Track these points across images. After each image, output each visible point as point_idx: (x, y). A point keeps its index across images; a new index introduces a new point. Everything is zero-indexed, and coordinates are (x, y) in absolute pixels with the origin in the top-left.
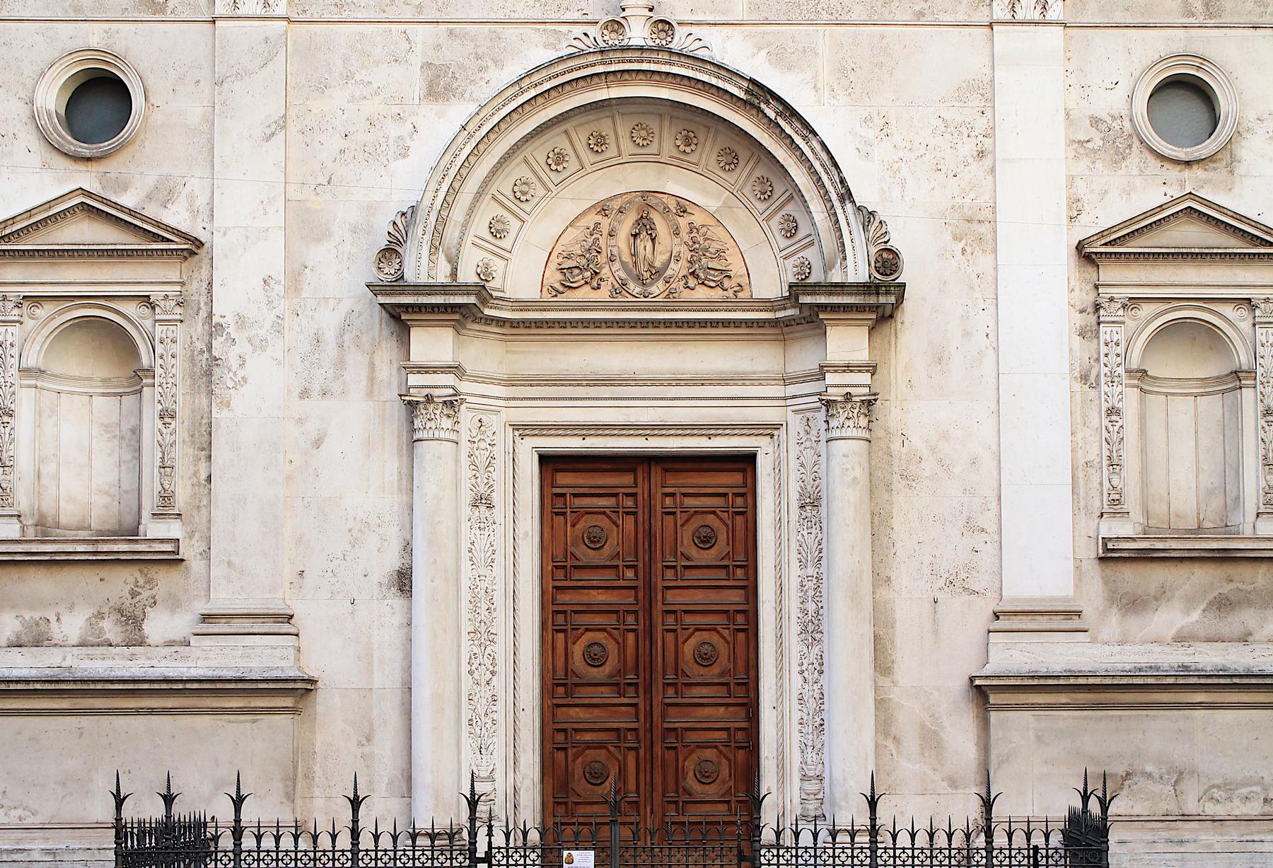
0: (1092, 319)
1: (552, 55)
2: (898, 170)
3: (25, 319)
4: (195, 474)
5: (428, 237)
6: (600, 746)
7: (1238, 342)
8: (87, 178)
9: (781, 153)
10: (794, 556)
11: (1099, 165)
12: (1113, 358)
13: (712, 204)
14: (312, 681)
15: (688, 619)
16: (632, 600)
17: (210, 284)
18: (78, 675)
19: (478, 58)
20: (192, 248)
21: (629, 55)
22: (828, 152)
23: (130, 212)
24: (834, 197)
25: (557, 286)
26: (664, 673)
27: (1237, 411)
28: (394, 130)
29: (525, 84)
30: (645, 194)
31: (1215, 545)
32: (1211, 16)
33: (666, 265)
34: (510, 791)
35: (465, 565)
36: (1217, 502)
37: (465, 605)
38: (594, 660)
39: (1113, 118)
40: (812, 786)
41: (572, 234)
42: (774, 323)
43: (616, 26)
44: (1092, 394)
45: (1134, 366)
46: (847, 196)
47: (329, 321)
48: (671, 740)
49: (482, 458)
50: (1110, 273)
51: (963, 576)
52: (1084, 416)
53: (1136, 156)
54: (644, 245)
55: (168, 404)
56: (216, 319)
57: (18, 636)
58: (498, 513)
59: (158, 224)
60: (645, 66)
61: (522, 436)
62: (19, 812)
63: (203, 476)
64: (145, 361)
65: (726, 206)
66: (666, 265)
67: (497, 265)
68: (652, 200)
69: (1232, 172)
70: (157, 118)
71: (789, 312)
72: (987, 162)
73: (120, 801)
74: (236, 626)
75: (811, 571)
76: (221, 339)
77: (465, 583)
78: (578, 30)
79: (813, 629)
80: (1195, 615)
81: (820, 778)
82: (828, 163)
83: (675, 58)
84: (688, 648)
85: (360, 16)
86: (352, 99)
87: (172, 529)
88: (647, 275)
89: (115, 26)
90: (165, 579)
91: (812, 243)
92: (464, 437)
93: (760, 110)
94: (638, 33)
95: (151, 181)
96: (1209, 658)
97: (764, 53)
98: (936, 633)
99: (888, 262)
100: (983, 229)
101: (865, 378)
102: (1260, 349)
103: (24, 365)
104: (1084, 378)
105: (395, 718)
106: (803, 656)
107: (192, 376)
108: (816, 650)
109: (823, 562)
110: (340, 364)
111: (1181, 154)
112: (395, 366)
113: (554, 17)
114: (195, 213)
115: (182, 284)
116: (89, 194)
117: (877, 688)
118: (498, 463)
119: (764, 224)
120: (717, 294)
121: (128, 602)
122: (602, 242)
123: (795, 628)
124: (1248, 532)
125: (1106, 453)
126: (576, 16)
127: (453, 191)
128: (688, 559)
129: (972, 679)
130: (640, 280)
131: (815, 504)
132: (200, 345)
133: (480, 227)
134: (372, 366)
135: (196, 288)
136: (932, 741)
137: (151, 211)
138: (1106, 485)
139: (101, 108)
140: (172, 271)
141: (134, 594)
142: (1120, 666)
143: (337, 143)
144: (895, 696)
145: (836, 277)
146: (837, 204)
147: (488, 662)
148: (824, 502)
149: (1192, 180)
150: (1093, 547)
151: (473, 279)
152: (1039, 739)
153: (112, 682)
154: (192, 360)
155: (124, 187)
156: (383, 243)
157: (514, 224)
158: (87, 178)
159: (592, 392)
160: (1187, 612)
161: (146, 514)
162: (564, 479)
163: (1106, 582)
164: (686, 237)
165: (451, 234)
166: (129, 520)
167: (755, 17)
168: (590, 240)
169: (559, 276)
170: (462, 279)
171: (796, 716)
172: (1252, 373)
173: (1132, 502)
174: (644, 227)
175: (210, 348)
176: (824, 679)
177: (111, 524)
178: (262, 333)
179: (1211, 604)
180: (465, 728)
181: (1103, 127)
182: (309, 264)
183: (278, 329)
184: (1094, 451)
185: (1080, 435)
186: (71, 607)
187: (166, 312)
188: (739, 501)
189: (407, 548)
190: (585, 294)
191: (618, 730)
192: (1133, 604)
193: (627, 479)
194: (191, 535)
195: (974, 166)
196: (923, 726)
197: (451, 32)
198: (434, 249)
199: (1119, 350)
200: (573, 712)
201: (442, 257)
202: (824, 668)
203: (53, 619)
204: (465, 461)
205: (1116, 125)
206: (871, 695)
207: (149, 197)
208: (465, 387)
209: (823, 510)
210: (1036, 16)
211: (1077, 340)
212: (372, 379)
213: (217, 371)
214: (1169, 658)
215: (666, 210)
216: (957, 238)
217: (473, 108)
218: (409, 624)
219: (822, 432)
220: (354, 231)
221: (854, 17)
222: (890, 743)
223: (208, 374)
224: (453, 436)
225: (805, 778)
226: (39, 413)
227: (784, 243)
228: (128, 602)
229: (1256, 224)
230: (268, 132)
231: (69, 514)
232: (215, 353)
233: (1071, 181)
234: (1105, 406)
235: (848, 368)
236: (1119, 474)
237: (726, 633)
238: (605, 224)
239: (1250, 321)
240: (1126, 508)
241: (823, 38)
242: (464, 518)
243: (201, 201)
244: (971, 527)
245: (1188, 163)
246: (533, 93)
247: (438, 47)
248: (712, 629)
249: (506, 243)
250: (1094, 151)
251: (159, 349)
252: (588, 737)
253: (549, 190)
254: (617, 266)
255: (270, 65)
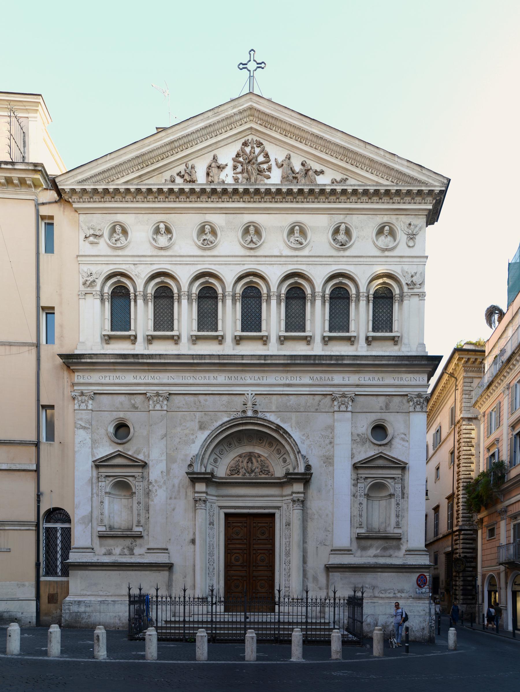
0: (356, 482)
1: (228, 419)
2: (311, 447)
3: (106, 481)
4: (145, 516)
5: (200, 462)
6: (238, 580)
7: (391, 488)
8: (120, 448)
9: (283, 442)
10: (284, 537)
11: (359, 445)
12: (361, 491)
13: (266, 455)
14: (173, 564)
15: (259, 551)
16: (245, 547)
17: (149, 473)
18: (119, 562)
19: (211, 420)
20: (144, 465)
21: (248, 419)
22: (295, 442)
23: (130, 456)
24: (296, 452)
25: (229, 474)
26: (253, 563)
27: (390, 504)
28: (192, 437)
29: (223, 425)
30: (250, 453)
31: (384, 535)
32: (387, 410)
33: (255, 469)
34: (217, 589)
35: (208, 538)
36: (384, 525)
37: (207, 547)
38: (237, 560)
39: (363, 434)
40: (287, 589)
41: (233, 462)
42: (280, 483)
43: (244, 412)
44: (356, 499)
45: (366, 493)
46: (299, 452)
47: (176, 482)
48: (254, 578)
49: (212, 513)
50: (360, 471)
51: (324, 541)
52: (354, 505)
53: (368, 444)
54: (250, 465)
55: (139, 500)
56: (150, 481)
57: (105, 553)
58: (215, 526)
59: (137, 459)
60: (251, 421)
61: (221, 509)
62: (106, 592)
63: (147, 517)
64: (134, 490)
65: (269, 455)
66: (255, 469)
67: (215, 469)
68: (252, 455)
69: (391, 447)
70: (136, 434)
71: (284, 480)
72: (332, 445)
73: (130, 589)
74: (155, 551)
75: (288, 540)
76: (151, 486)
77: (208, 542)
78: (236, 413)
79: (288, 554)
80: (378, 551)
81: (289, 587)
82: (295, 444)
83: (259, 419)
84: (259, 558)
85: (184, 410)
86: (182, 430)
87: (140, 529)
88: (250, 472)
89: (126, 412)
90: (139, 541)
91: (290, 464)
92: (208, 509)
93: (279, 432)
94: (250, 414)
95: (135, 448)
96: (382, 561)
97: (279, 419)
98: (317, 554)
99: (308, 467)
100: (330, 461)
101: (302, 495)
102: (396, 489)
103: (106, 491)
104: (354, 496)
105: (191, 573)
106: (285, 560)
107: (145, 494)
108: (289, 558)
109: (291, 538)
110: (179, 491)
111: (379, 443)
112: (192, 492)
113: (229, 410)
114: (145, 456)
115: (142, 473)
116: (121, 452)
117: (303, 567)
118: (215, 515)
119: (278, 460)
120: (267, 476)
121: (130, 545)
122: (240, 464)
123: (284, 553)
124: (392, 532)
125: (358, 513)
126: (235, 410)
127: (206, 451)
128: (259, 537)
129: (325, 565)
130: (248, 473)
131: (289, 525)
132: (146, 487)
133: (212, 460)
134: (186, 492)
135: (145, 474)
136: (315, 579)
137: (135, 456)
138: (358, 520)
139: (122, 431)
140: (140, 470)
141: (131, 544)
142: (361, 562)
143: (178, 440)
144: (307, 569)
145: (296, 471)
146: (297, 454)
147: (213, 560)
148: (291, 524)
149: (381, 449)
150: (355, 535)
151: (209, 471)
152: (341, 579)
153: (127, 563)
154: (145, 490)
155: (129, 450)
156: (189, 463)
157: (219, 459)
158: (120, 448)
159: (237, 499)
160: (377, 550)
161: (134, 526)
162: (231, 519)
163: (357, 543)
164: (260, 463)
165: (205, 461)
166: (130, 527)
167: (277, 410)
168: (237, 463)
169: (230, 472)
170: (207, 471)
171: (284, 573)
172: (394, 495)
173: (364, 525)
174: (250, 460)
175: (149, 488)
176: (291, 565)
177: (126, 528)
178: (161, 484)
179: (382, 548)
180: (207, 575)
181: (360, 436)
182: (172, 468)
183: (165, 483)
184: (356, 513)
185: (352, 509)
186: (117, 546)
187: (138, 479)
188: (271, 524)
189: (194, 534)
190: (236, 476)
191: (242, 576)
192: (364, 549)
193: (245, 519)
194: (144, 530)
195: (329, 446)
196: (313, 576)
197: (205, 414)
198: (201, 464)
199: (363, 489)
200: (232, 572)
201: (203, 466)
202: (291, 562)
203: (113, 549)
204: (208, 514)
205: (363, 436)
206: (302, 568)
207: (134, 453)
208: (208, 497)
209: (291, 526)
210: (345, 410)
211: (352, 487)
212: (186, 495)
213: (150, 493)
214: (372, 561)
215: (255, 457)
216: (324, 463)
217: (210, 432)
218: (195, 551)
219: (292, 508)
220: (182, 460)
221: (301, 410)
222: (306, 580)
223: (148, 494)
224: (205, 508)
225: (285, 587)
226: (109, 502)
227: (283, 464)
228: (130, 545)
229: (397, 459)
230: (162, 437)
231: (116, 525)
232: (150, 489)
233: (352, 449)
234: (358, 502)
235: (298, 493)
236: (361, 518)
237: (267, 554)
238: (241, 459)
239: (394, 483)
240: (363, 526)
241: (294, 415)
242: (207, 527)
243: (146, 453)
244: (326, 530)
245: (380, 445)
246: (225, 428)
247: (202, 417)
248: (264, 553)
249: (217, 464)
250: (358, 442)
251: (137, 488)
252: (235, 578)
253: (227, 452)
254: (243, 469)
255: (162, 422)
